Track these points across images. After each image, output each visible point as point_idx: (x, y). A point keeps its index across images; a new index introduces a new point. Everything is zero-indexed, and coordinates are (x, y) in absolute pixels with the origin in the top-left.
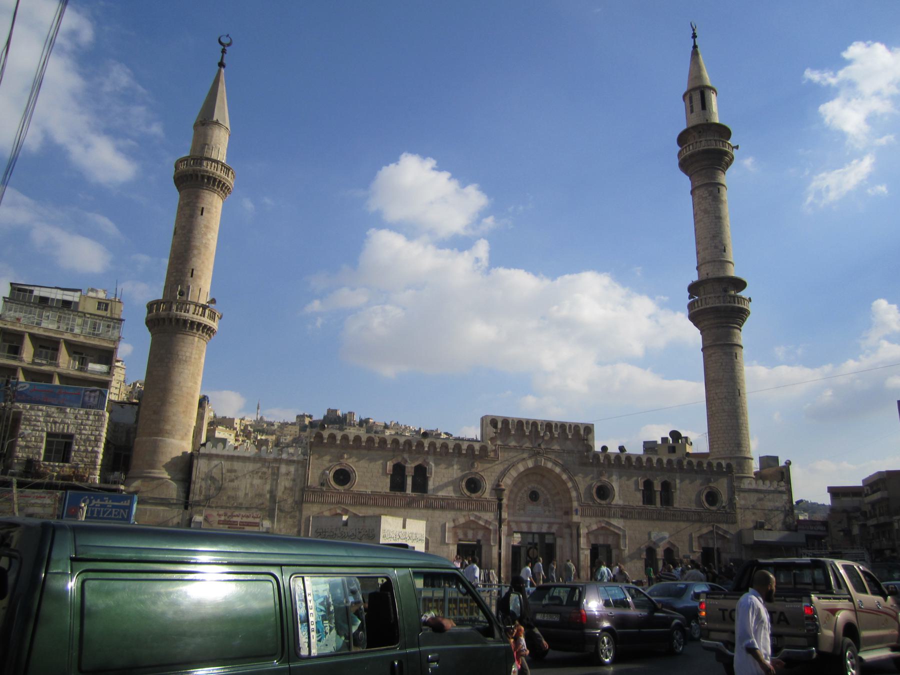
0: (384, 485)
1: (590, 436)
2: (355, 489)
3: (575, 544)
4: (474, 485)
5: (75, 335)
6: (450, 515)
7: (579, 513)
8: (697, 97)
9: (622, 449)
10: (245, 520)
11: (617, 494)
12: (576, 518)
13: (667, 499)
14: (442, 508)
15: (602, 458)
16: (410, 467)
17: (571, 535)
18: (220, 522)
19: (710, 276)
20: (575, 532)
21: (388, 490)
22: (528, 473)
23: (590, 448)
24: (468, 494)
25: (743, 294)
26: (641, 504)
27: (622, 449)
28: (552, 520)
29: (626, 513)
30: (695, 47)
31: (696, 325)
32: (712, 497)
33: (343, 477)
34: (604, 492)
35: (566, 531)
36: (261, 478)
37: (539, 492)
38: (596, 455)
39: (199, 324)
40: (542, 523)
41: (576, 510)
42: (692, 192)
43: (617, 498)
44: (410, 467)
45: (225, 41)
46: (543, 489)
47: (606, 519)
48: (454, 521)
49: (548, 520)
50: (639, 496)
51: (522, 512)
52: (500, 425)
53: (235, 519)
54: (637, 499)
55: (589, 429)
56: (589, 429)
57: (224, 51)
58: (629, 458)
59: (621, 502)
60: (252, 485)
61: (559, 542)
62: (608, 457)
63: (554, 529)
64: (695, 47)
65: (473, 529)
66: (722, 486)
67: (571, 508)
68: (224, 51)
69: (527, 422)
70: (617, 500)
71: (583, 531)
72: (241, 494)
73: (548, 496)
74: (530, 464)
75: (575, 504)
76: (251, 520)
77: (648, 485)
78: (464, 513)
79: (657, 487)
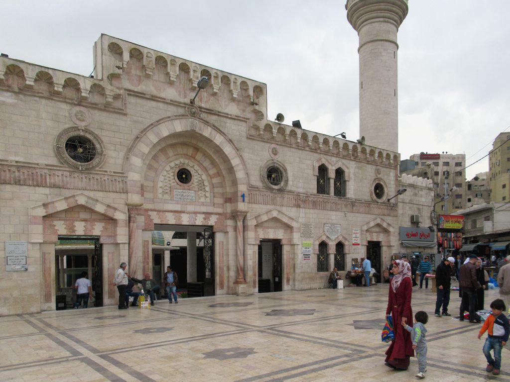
1: (261, 100)
3: (240, 240)
7: (246, 199)
9: (297, 124)
12: (242, 206)
13: (340, 191)
15: (275, 131)
17: (235, 228)
20: (240, 224)
23: (260, 115)
26: (315, 191)
27: (297, 124)
28: (210, 209)
29: (300, 201)
34: (274, 174)
35: (230, 223)
37: (193, 173)
38: (268, 127)
40: (196, 213)
41: (243, 196)
46: (196, 167)
47: (279, 208)
48: (45, 205)
49: (204, 209)
51: (167, 197)
58: (305, 135)
61: (219, 237)
62: (282, 130)
63: (212, 221)
65: (85, 220)
67: (236, 193)
71: (252, 223)
73: (204, 177)
74: (179, 126)
75: (242, 188)
77: (323, 170)
78: (67, 193)
79: (332, 174)
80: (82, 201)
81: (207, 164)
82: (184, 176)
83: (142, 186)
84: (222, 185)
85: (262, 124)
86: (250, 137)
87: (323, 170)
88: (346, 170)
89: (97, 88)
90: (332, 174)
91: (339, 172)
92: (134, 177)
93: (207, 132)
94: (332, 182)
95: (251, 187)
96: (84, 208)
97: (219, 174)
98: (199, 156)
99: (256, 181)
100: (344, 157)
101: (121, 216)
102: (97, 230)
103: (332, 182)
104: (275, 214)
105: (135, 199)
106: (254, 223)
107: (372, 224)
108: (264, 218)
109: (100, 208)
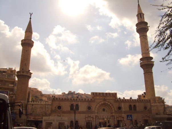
0: (69, 109)
2: (63, 110)
4: (89, 108)
5: (6, 79)
6: (84, 115)
8: (139, 16)
9: (124, 98)
10: (38, 118)
11: (123, 108)
14: (82, 113)
16: (75, 104)
17: (113, 118)
18: (33, 119)
19: (144, 57)
20: (113, 117)
21: (70, 110)
22: (102, 105)
24: (88, 110)
25: (152, 60)
28: (108, 115)
29: (125, 112)
30: (139, 4)
31: (142, 68)
32: (145, 108)
33: (59, 107)
34: (120, 108)
35: (112, 117)
36: (42, 109)
38: (118, 100)
39: (27, 76)
40: (106, 116)
42: (140, 37)
43: (123, 109)
44: (75, 104)
45: (31, 13)
50: (128, 108)
52: (95, 94)
53: (36, 118)
54: (128, 109)
55: (116, 94)
56: (116, 94)
57: (31, 16)
59: (124, 110)
60: (40, 110)
64: (139, 4)
66: (148, 105)
68: (31, 16)
69: (101, 93)
70: (123, 110)
71: (115, 117)
72: (38, 112)
76: (39, 118)
77: (130, 106)
78: (87, 114)
79: (133, 106)
80: (89, 115)
81: (107, 107)
82: (104, 110)
83: (97, 112)
84: (110, 111)
85: (116, 100)
86: (115, 102)
87: (130, 106)
88: (136, 105)
89: (91, 100)
90: (133, 106)
91: (135, 106)
92: (96, 111)
93: (107, 102)
94: (133, 108)
95: (115, 111)
96: (90, 116)
97: (110, 109)
98: (106, 106)
99: (116, 110)
100: (135, 102)
101: (94, 117)
102: (91, 119)
103: (133, 108)
104: (120, 115)
105: (96, 114)
106: (116, 117)
107: (144, 116)
108: (118, 116)
109: (92, 116)
